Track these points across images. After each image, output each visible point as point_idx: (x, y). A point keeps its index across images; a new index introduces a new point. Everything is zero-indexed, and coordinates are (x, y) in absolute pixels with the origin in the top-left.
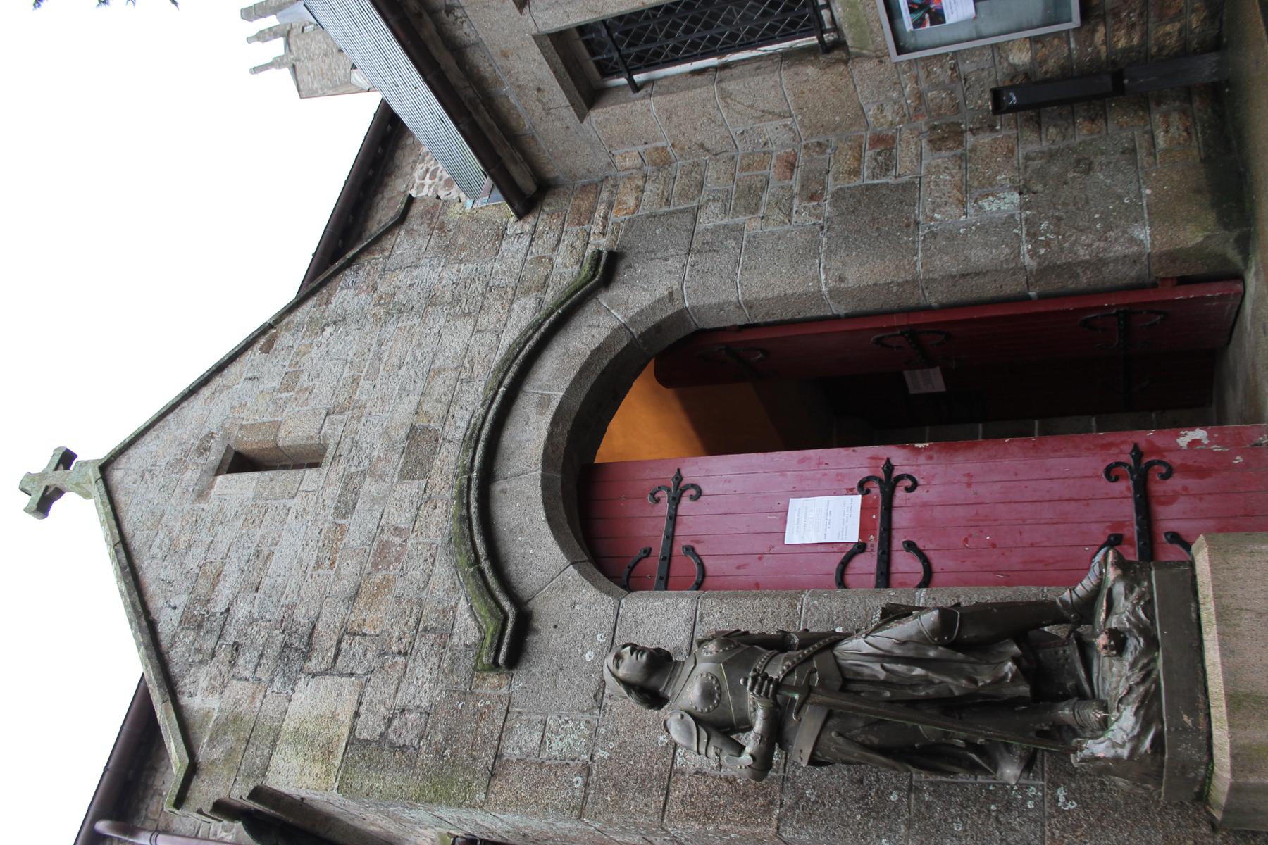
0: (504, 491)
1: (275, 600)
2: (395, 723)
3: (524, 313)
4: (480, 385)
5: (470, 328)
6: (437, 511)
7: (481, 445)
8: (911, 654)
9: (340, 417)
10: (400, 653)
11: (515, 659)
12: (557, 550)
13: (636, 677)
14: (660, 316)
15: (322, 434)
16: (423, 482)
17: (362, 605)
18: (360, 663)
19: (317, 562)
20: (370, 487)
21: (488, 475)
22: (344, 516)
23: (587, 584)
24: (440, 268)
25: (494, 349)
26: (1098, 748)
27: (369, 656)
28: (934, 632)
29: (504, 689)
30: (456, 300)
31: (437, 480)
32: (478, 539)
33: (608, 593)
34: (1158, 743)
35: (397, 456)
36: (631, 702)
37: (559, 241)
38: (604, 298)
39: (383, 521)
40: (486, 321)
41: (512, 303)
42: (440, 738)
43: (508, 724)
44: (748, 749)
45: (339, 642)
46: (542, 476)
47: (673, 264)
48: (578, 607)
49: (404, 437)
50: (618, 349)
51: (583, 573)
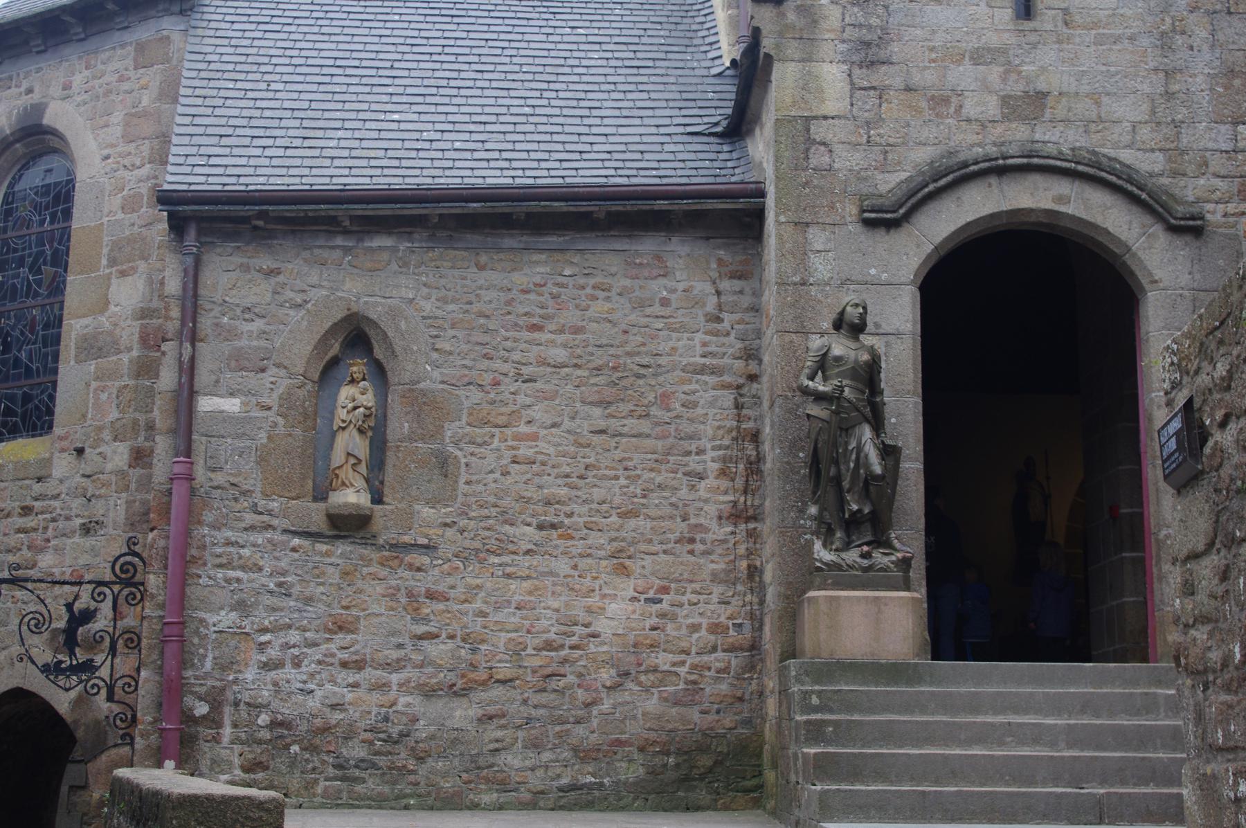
0: (990, 185)
1: (903, 21)
2: (822, 148)
3: (1148, 163)
4: (1082, 142)
5: (1139, 119)
6: (975, 136)
7: (1025, 161)
8: (861, 461)
9: (1060, 24)
10: (869, 137)
11: (869, 224)
12: (945, 234)
13: (847, 317)
14: (1139, 274)
15: (1046, 11)
16: (999, 117)
17: (902, 97)
18: (860, 109)
19: (934, 47)
20: (994, 73)
21: (1002, 171)
22: (971, 58)
23: (921, 261)
24: (1206, 71)
25: (1116, 146)
26: (818, 545)
27: (866, 114)
28: (871, 472)
29: (849, 219)
30: (1169, 95)
31: (999, 129)
32: (950, 178)
33: (915, 275)
34: (819, 569)
35: (1022, 89)
36: (834, 316)
37: (1223, 177)
38: (1157, 229)
39: (966, 93)
40: (1145, 133)
41: (1160, 150)
42: (816, 182)
43: (827, 226)
44: (811, 383)
45: (874, 88)
46: (1002, 212)
47: (1185, 279)
48: (905, 257)
49: (1039, 89)
50: (1111, 247)
51: (929, 256)
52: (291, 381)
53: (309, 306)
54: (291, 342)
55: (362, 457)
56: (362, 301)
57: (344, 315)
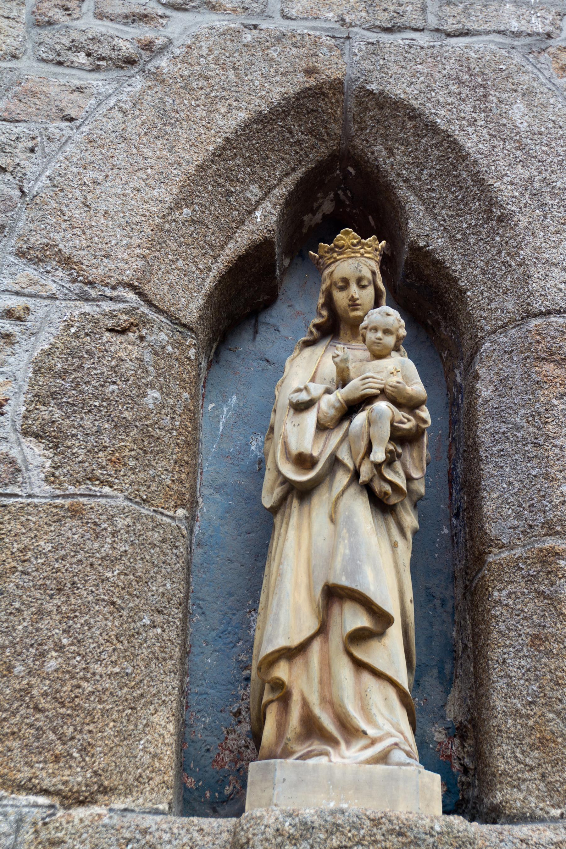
52: (87, 308)
53: (163, 62)
54: (89, 175)
55: (393, 609)
56: (358, 46)
57: (292, 90)
